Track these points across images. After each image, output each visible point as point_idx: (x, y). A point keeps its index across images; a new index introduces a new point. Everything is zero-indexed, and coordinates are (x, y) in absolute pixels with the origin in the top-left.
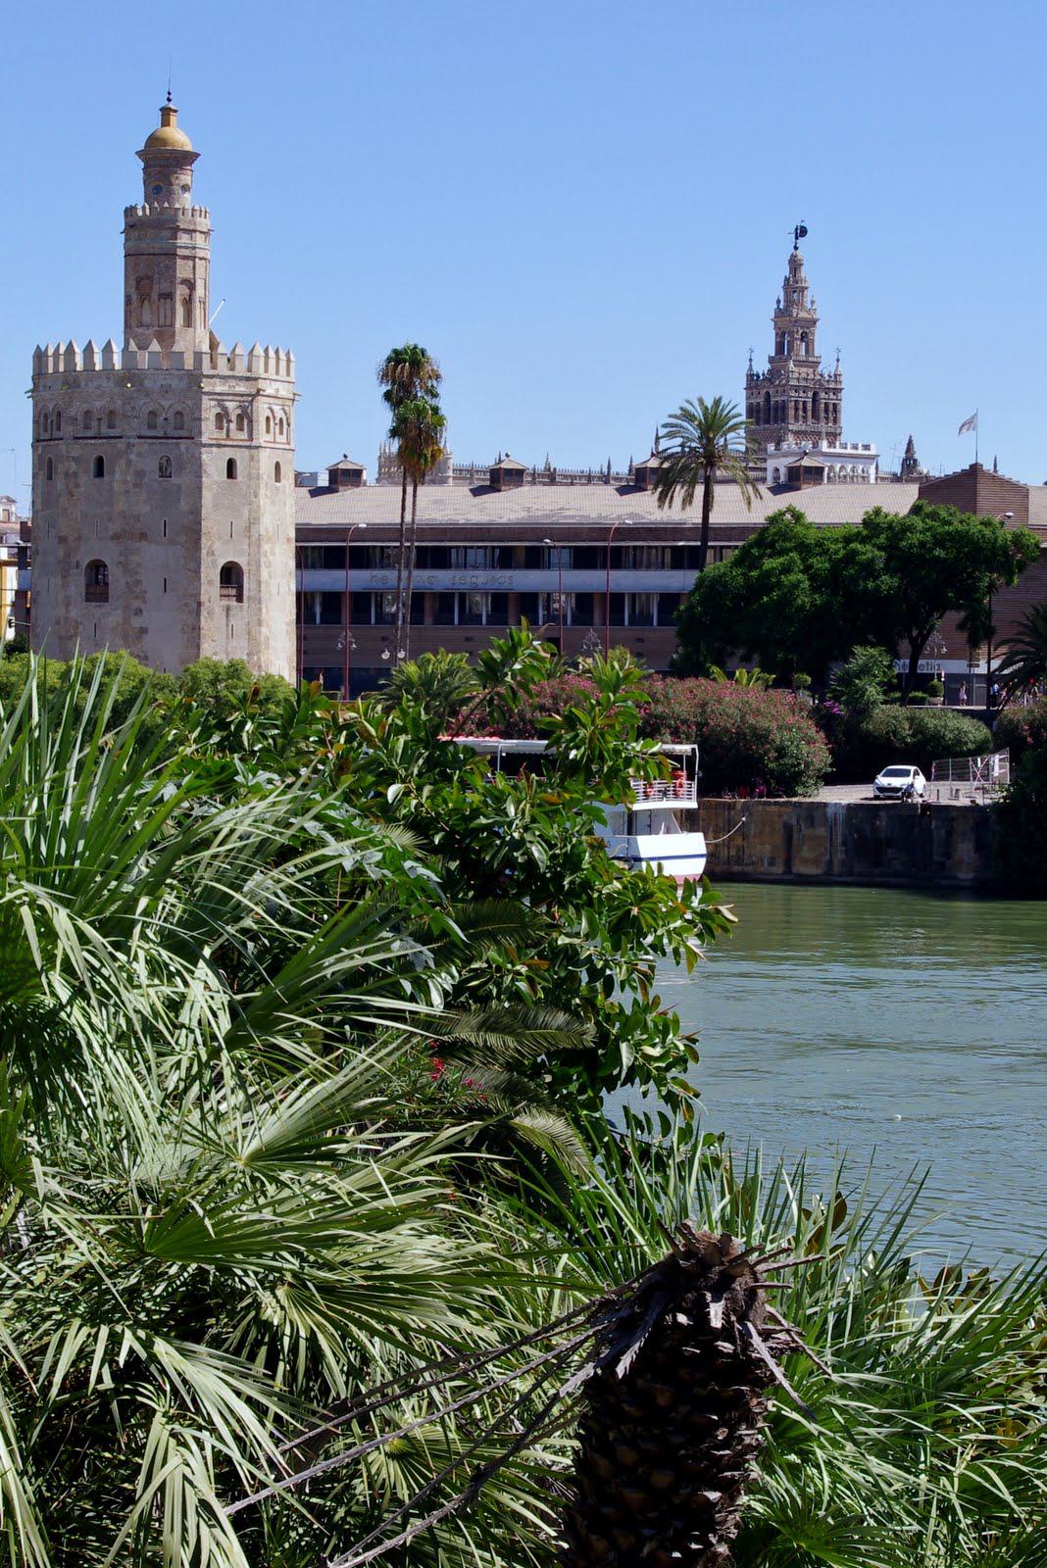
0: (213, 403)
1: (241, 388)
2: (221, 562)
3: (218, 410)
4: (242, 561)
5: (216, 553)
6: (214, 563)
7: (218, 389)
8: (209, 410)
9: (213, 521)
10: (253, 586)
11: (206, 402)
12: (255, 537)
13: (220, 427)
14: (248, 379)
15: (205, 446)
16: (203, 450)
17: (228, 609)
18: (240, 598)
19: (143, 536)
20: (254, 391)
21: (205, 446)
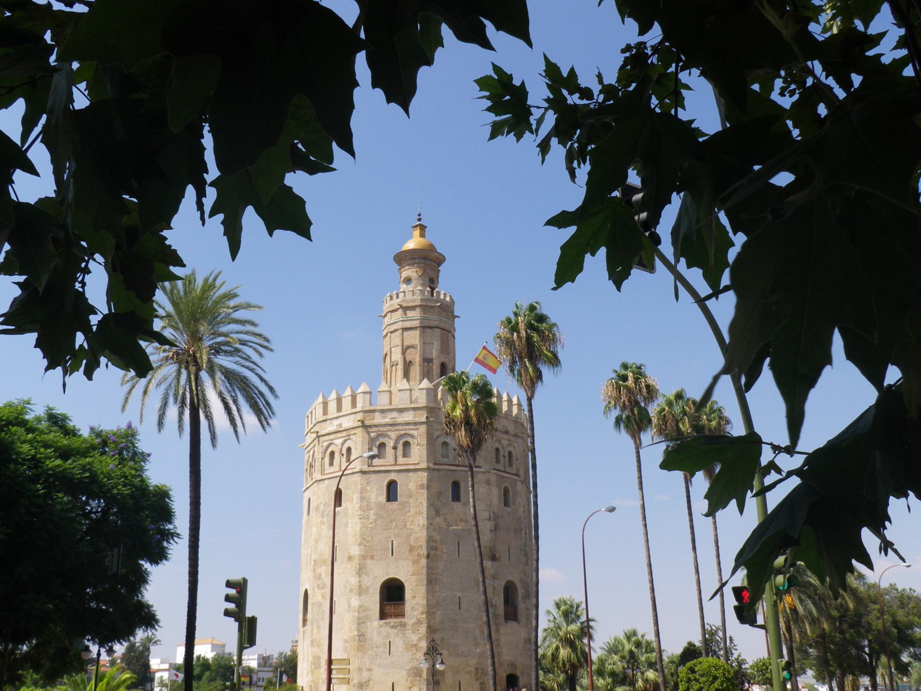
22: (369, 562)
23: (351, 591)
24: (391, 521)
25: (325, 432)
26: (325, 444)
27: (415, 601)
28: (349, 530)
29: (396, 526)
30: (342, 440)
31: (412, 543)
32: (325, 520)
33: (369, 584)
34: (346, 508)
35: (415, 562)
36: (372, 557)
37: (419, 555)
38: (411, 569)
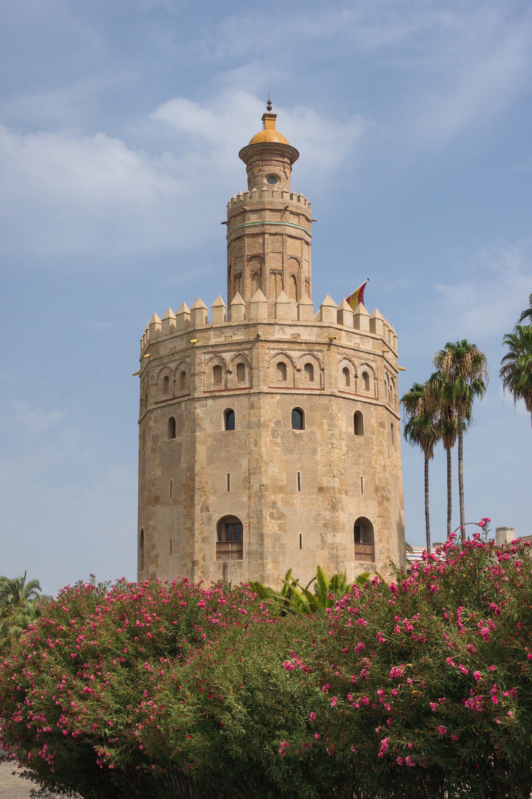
0: (208, 356)
1: (239, 337)
2: (217, 517)
3: (216, 362)
4: (242, 515)
5: (214, 505)
6: (209, 519)
7: (212, 342)
8: (204, 363)
9: (209, 473)
10: (254, 540)
11: (202, 357)
12: (256, 487)
13: (218, 380)
14: (246, 326)
15: (199, 399)
16: (197, 404)
17: (225, 566)
18: (240, 553)
19: (157, 500)
20: (252, 338)
21: (199, 399)
22: (344, 496)
23: (325, 525)
24: (359, 457)
25: (272, 338)
26: (273, 352)
27: (381, 545)
28: (318, 457)
29: (364, 462)
30: (302, 353)
31: (377, 482)
32: (279, 440)
33: (345, 521)
34: (312, 433)
35: (380, 503)
36: (346, 493)
37: (382, 496)
38: (377, 510)
